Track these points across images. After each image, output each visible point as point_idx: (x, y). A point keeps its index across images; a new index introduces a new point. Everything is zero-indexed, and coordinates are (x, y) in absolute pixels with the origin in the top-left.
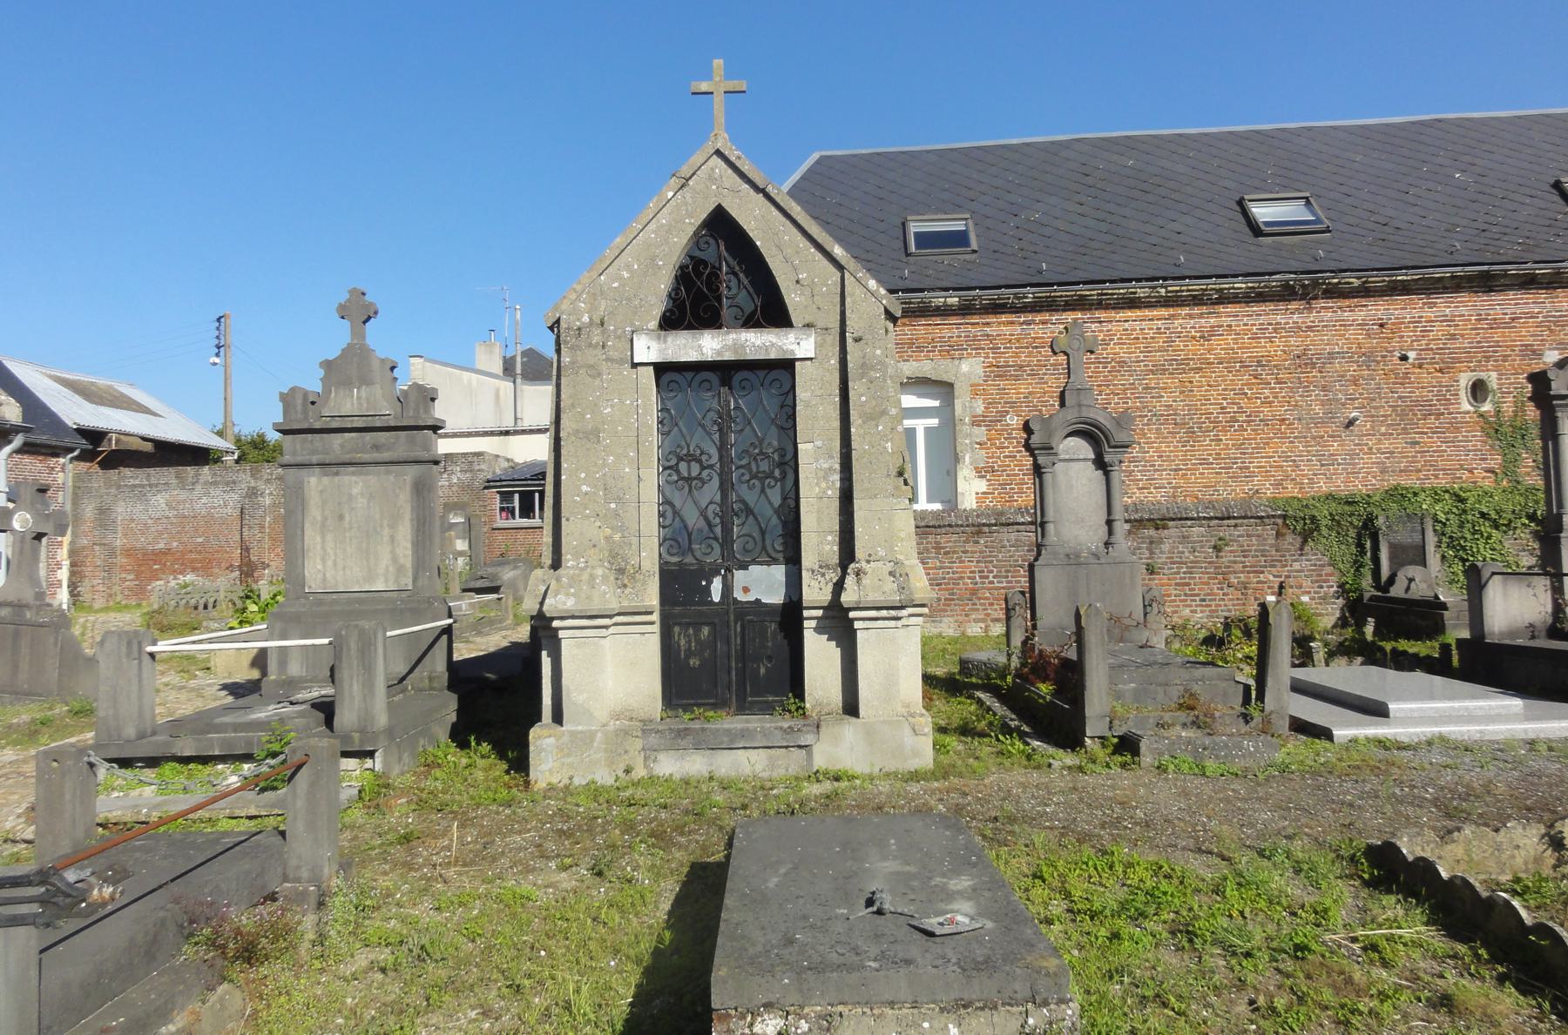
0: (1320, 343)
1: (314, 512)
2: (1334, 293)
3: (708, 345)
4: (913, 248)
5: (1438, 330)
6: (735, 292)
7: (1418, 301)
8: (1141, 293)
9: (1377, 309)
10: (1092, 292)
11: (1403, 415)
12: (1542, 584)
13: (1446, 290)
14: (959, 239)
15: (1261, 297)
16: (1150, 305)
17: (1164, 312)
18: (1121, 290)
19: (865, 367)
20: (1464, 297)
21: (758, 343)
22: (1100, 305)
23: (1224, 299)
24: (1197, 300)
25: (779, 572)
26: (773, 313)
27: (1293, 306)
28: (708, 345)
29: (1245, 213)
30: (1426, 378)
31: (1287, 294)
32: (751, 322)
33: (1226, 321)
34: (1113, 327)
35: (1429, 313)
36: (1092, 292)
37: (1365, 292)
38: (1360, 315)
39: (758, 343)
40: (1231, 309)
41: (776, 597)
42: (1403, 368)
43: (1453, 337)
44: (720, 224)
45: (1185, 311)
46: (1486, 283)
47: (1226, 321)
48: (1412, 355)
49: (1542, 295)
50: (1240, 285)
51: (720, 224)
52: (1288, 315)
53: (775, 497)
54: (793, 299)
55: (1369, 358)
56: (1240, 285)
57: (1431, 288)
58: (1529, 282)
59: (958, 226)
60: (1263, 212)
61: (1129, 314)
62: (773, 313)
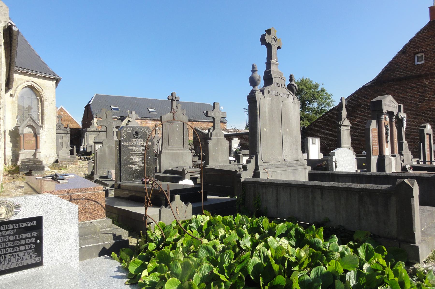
1: (90, 138)
4: (113, 110)
14: (117, 109)
15: (150, 120)
16: (140, 120)
17: (141, 121)
23: (147, 120)
24: (144, 120)
29: (148, 110)
31: (153, 120)
33: (147, 122)
40: (148, 121)
45: (143, 121)
47: (147, 122)
50: (149, 119)
56: (149, 119)
59: (117, 108)
60: (151, 110)
61: (138, 120)
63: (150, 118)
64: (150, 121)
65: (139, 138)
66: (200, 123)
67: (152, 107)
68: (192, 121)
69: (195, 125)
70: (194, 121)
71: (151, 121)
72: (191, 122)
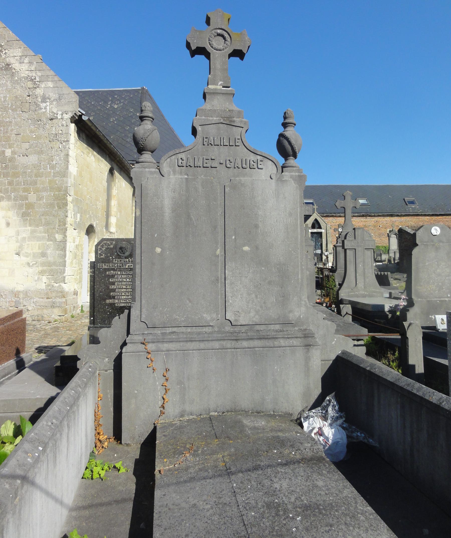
0: (367, 224)
2: (370, 216)
3: (315, 230)
5: (385, 222)
6: (317, 226)
7: (382, 218)
8: (341, 215)
9: (376, 219)
10: (334, 215)
11: (379, 235)
12: (388, 255)
13: (386, 216)
15: (359, 216)
18: (339, 214)
19: (329, 233)
20: (388, 217)
21: (319, 230)
22: (336, 217)
25: (320, 251)
26: (320, 227)
27: (364, 218)
28: (315, 230)
30: (383, 230)
31: (363, 216)
32: (318, 228)
34: (337, 220)
35: (384, 220)
36: (334, 215)
37: (374, 216)
38: (374, 219)
39: (319, 230)
41: (320, 253)
42: (379, 228)
43: (387, 223)
44: (316, 220)
46: (392, 216)
48: (381, 226)
49: (400, 218)
50: (356, 214)
51: (316, 220)
52: (363, 219)
53: (320, 244)
54: (322, 227)
55: (375, 226)
56: (356, 214)
57: (384, 216)
58: (398, 216)
59: (311, 201)
62: (320, 227)
63: (358, 214)
64: (358, 218)
65: (126, 258)
66: (445, 218)
67: (362, 198)
68: (429, 214)
69: (436, 220)
70: (433, 215)
71: (360, 218)
72: (428, 217)
